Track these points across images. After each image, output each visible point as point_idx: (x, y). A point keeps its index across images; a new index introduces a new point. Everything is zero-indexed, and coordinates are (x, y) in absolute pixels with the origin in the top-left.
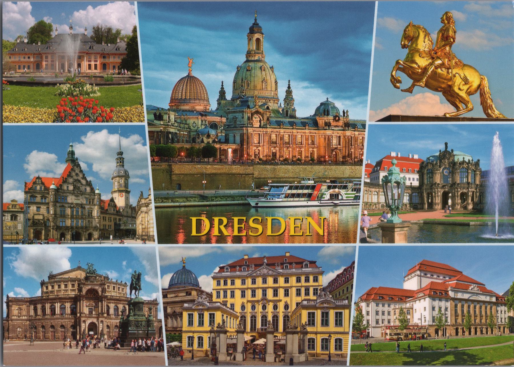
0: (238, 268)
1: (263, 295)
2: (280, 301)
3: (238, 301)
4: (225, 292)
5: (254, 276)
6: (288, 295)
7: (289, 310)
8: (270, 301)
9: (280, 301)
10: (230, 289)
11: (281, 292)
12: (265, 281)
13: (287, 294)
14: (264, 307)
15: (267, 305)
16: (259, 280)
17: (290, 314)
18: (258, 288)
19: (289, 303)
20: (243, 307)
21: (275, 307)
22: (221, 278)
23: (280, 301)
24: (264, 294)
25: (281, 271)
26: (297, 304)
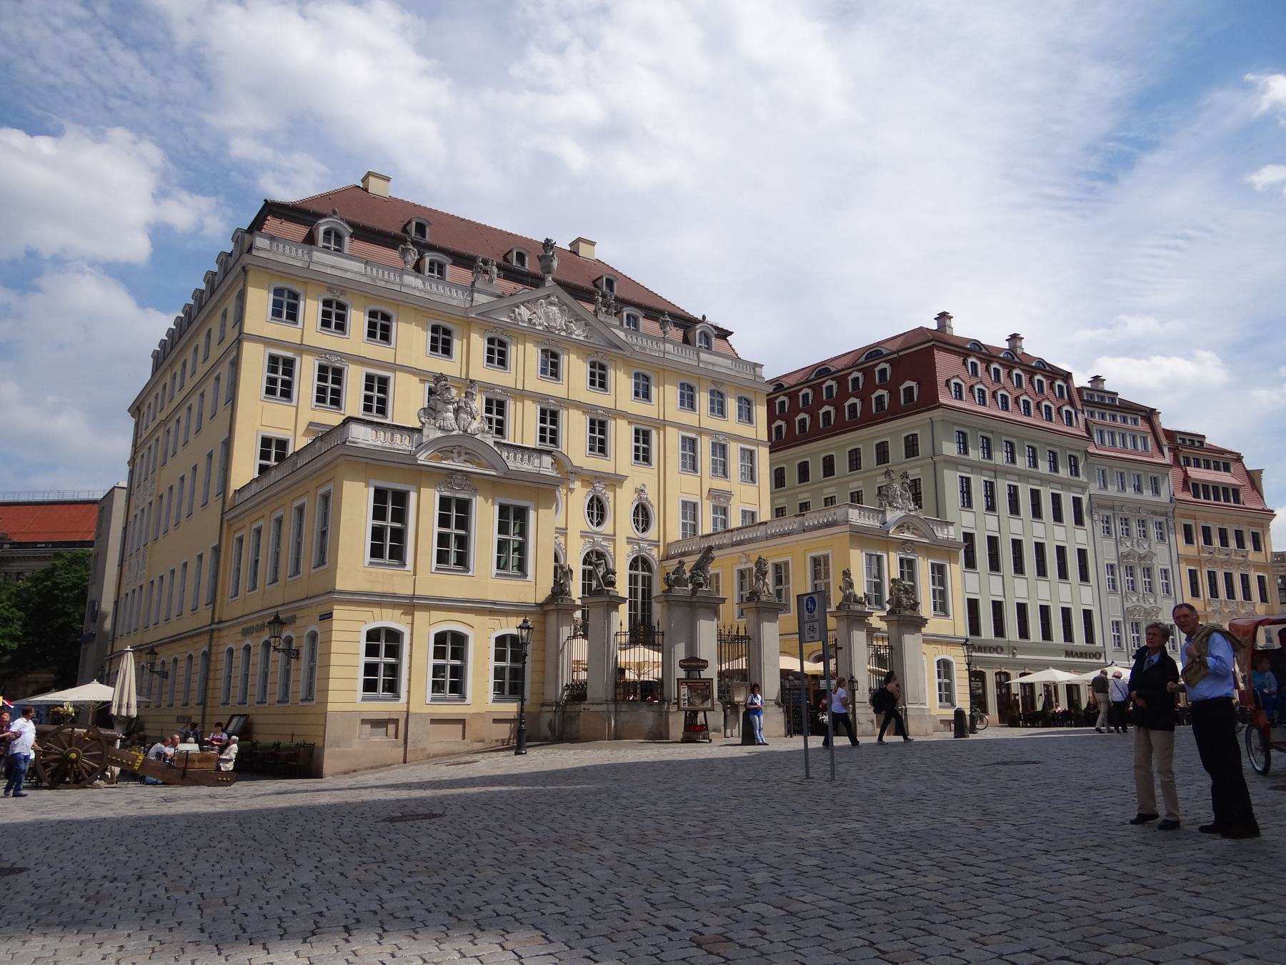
2: (615, 481)
5: (503, 327)
7: (652, 534)
12: (551, 366)
13: (642, 455)
17: (654, 554)
18: (522, 395)
19: (651, 496)
21: (597, 510)
22: (305, 282)
25: (622, 335)
26: (690, 509)
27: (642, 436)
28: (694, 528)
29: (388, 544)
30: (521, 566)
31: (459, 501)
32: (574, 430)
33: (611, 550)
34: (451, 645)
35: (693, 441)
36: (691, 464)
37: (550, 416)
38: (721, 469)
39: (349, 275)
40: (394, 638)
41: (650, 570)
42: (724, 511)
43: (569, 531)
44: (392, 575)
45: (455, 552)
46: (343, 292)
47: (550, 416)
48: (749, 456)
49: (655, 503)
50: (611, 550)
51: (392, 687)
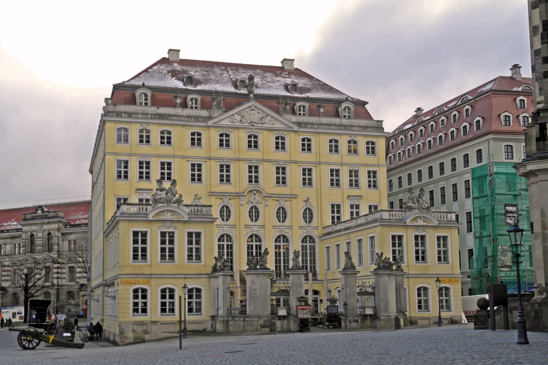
1: (250, 181)
7: (315, 222)
8: (270, 196)
10: (159, 156)
11: (294, 175)
13: (307, 182)
14: (254, 214)
15: (260, 207)
17: (315, 234)
19: (313, 204)
21: (282, 214)
23: (294, 196)
24: (254, 179)
26: (336, 208)
27: (307, 172)
28: (339, 218)
29: (140, 254)
30: (198, 258)
31: (169, 233)
32: (267, 174)
33: (290, 234)
34: (168, 293)
35: (337, 171)
36: (335, 183)
37: (253, 169)
38: (354, 184)
40: (144, 291)
41: (314, 242)
42: (357, 207)
43: (266, 227)
44: (142, 266)
45: (167, 254)
46: (148, 125)
47: (253, 169)
48: (372, 174)
49: (315, 206)
50: (290, 234)
51: (144, 311)
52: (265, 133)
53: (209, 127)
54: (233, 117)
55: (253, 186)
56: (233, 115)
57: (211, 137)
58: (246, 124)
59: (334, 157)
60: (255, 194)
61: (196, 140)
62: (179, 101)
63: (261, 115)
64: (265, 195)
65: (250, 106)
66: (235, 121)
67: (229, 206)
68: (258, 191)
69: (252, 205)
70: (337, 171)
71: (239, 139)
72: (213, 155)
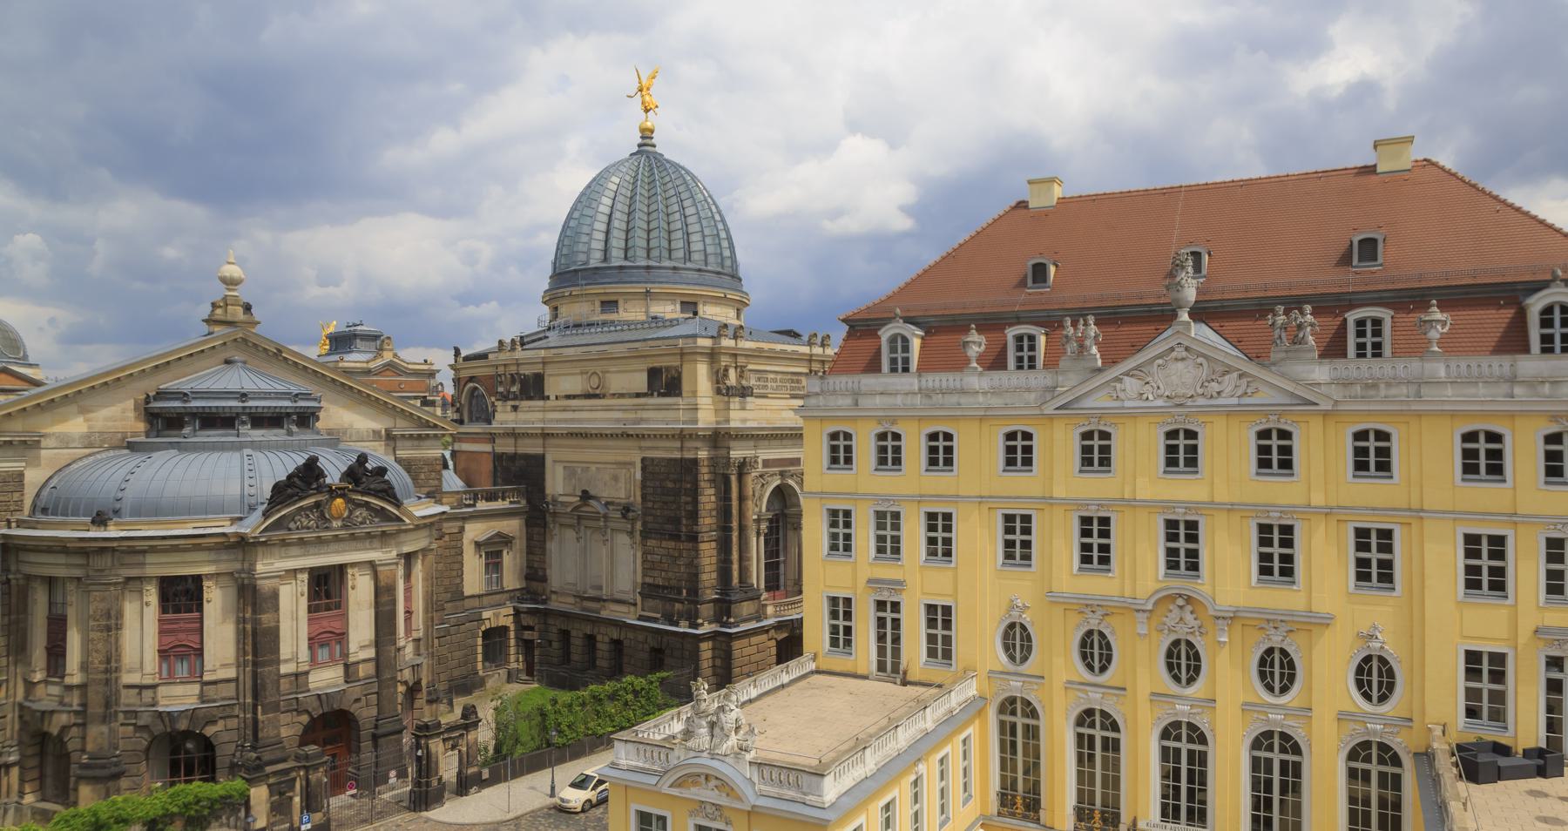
0: (977, 344)
1: (1172, 565)
3: (981, 587)
4: (888, 521)
6: (1386, 577)
8: (1232, 618)
9: (1318, 622)
12: (1181, 452)
14: (1184, 662)
16: (1140, 449)
20: (1017, 640)
21: (1277, 670)
25: (1321, 372)
35: (1498, 542)
39: (899, 400)
52: (1220, 424)
53: (1050, 417)
54: (1118, 386)
55: (1181, 583)
56: (1118, 380)
57: (1058, 447)
58: (1160, 402)
59: (1484, 495)
60: (1181, 607)
61: (1019, 452)
62: (974, 351)
63: (1204, 373)
64: (1211, 613)
65: (1172, 349)
66: (1122, 395)
67: (1106, 632)
68: (1189, 600)
69: (1173, 637)
70: (1498, 542)
71: (1140, 449)
72: (1059, 492)
